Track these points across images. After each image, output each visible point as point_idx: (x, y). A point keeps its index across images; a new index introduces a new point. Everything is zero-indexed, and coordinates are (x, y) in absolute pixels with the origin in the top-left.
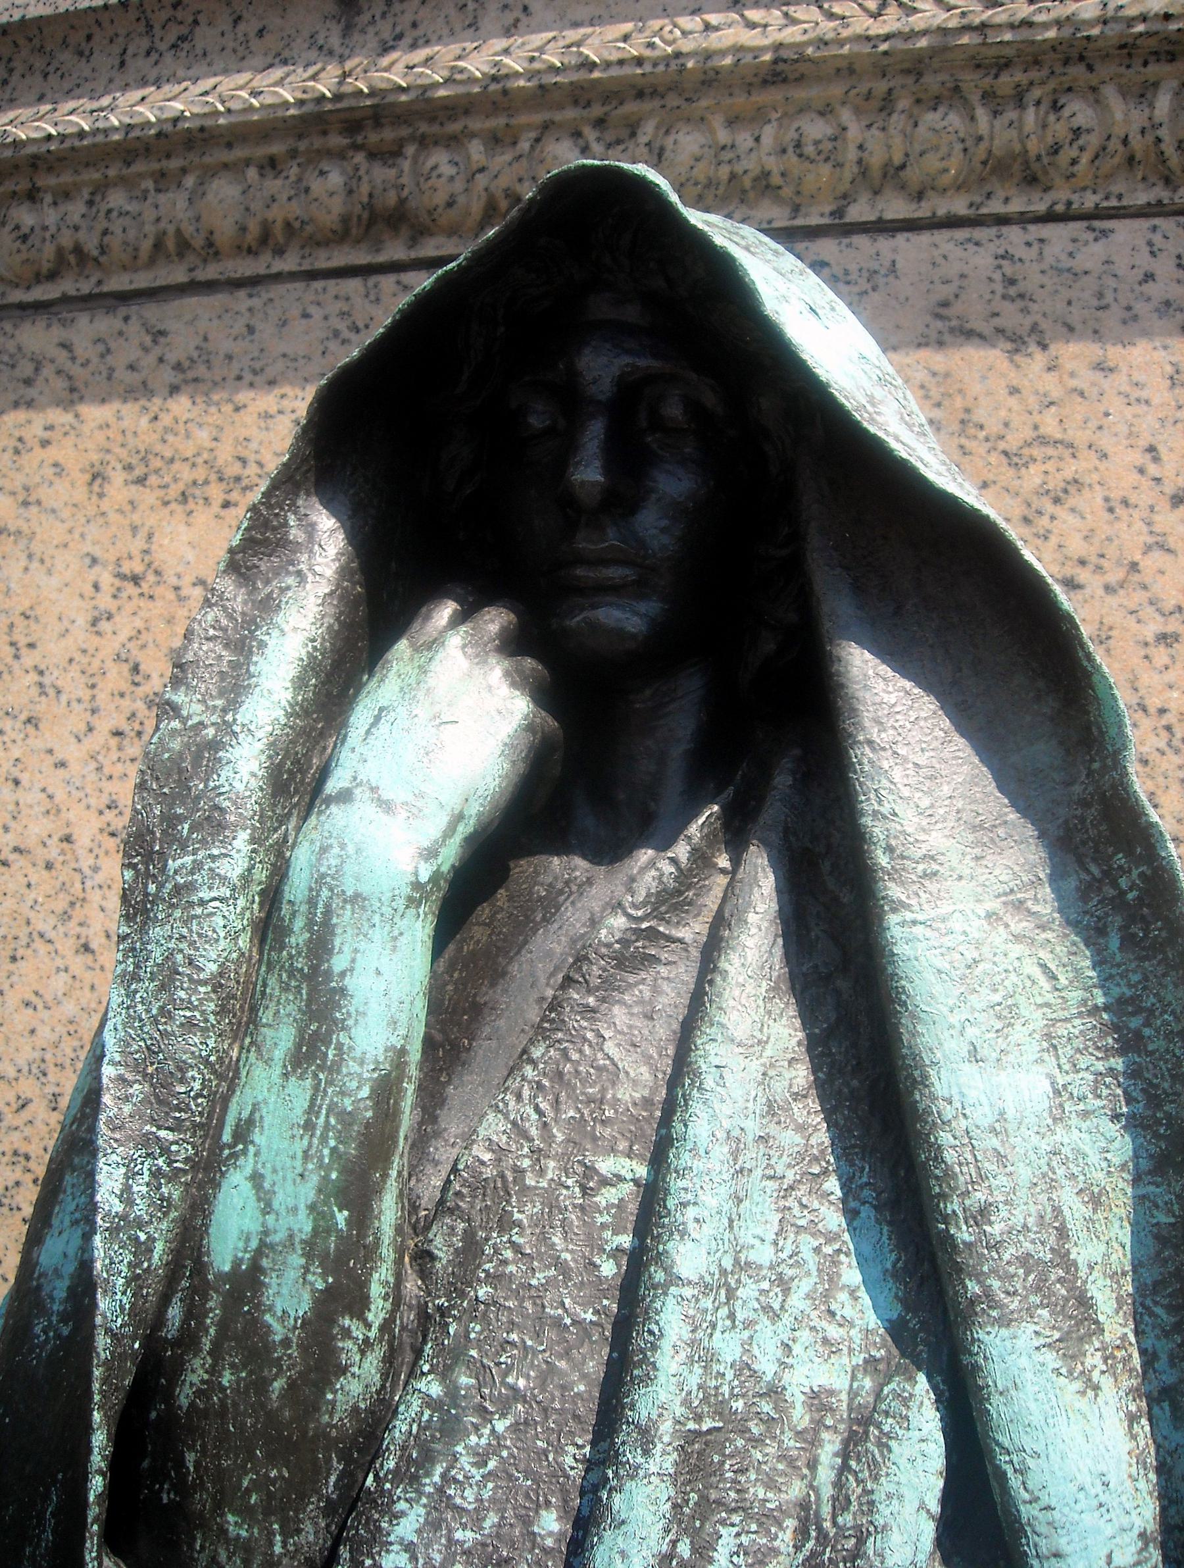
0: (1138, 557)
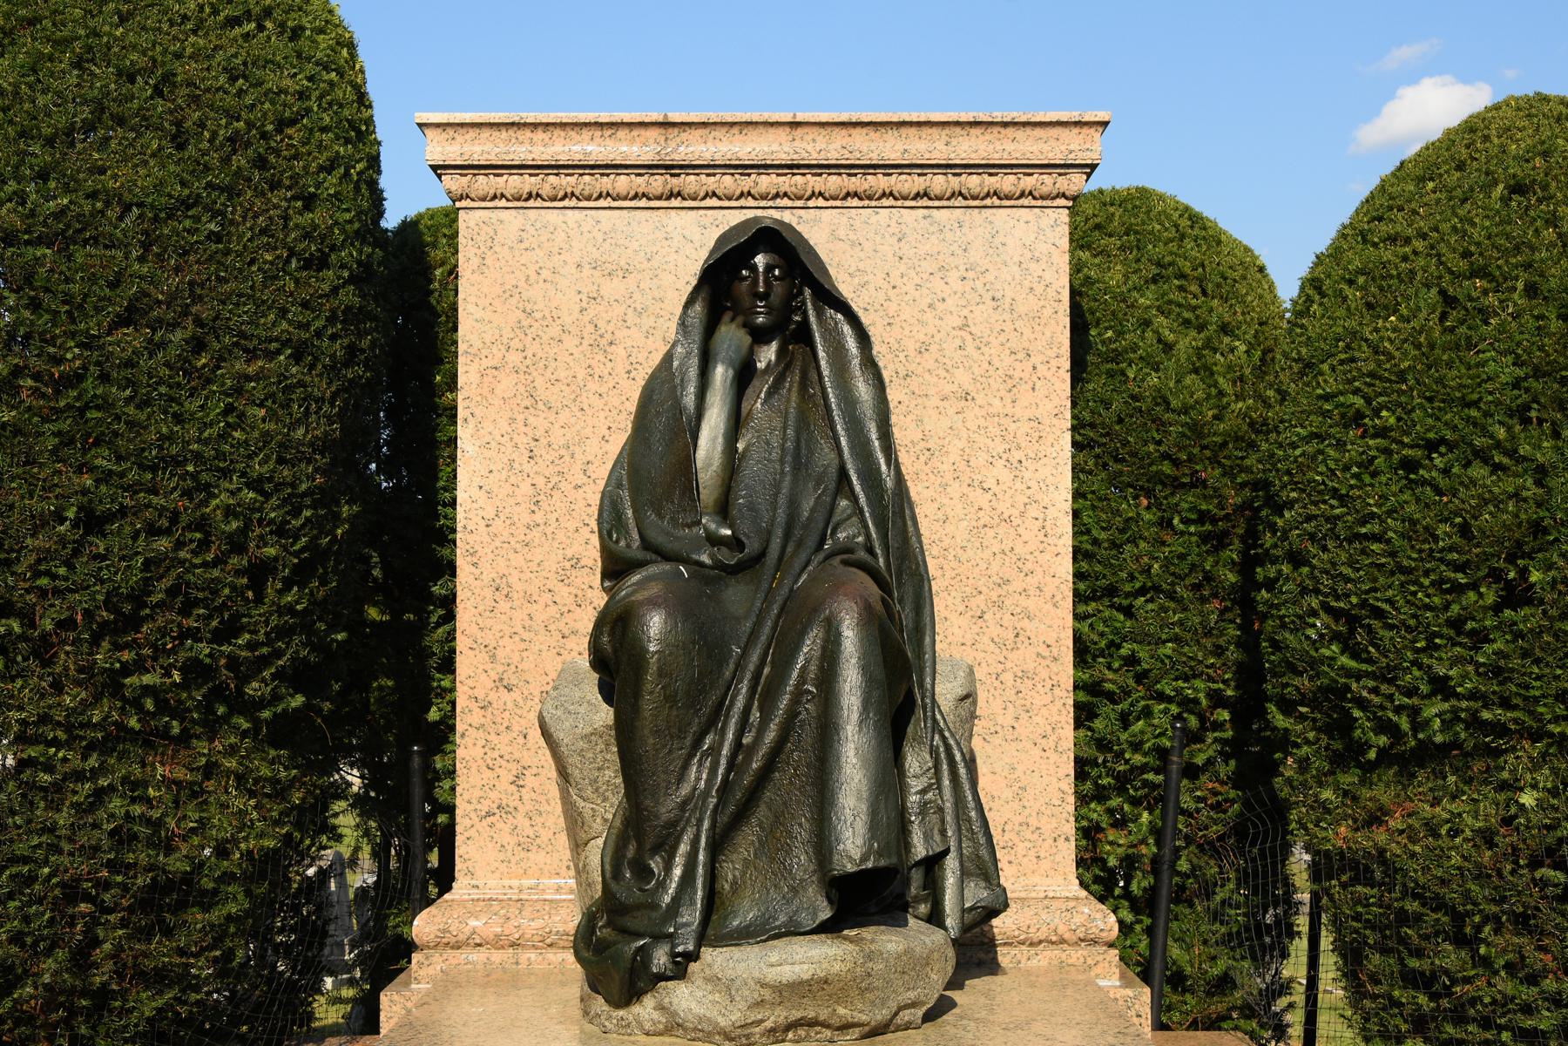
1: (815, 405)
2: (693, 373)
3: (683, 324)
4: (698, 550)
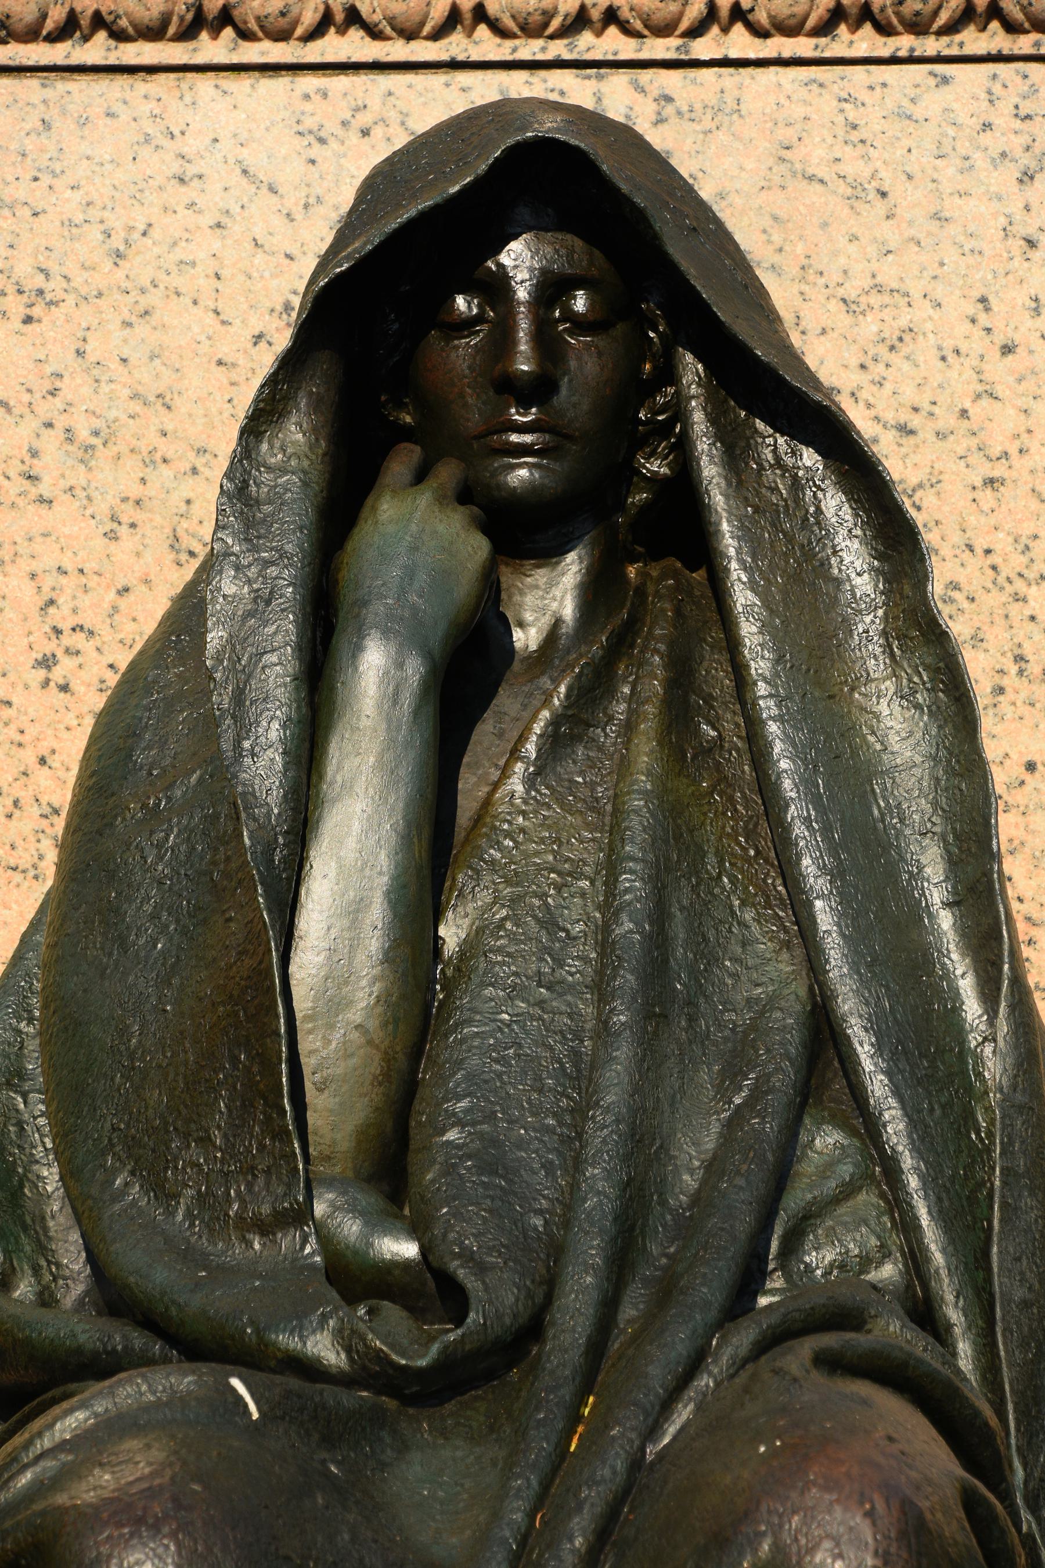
0: (967, 405)
1: (723, 782)
2: (278, 673)
3: (239, 491)
4: (298, 1318)
